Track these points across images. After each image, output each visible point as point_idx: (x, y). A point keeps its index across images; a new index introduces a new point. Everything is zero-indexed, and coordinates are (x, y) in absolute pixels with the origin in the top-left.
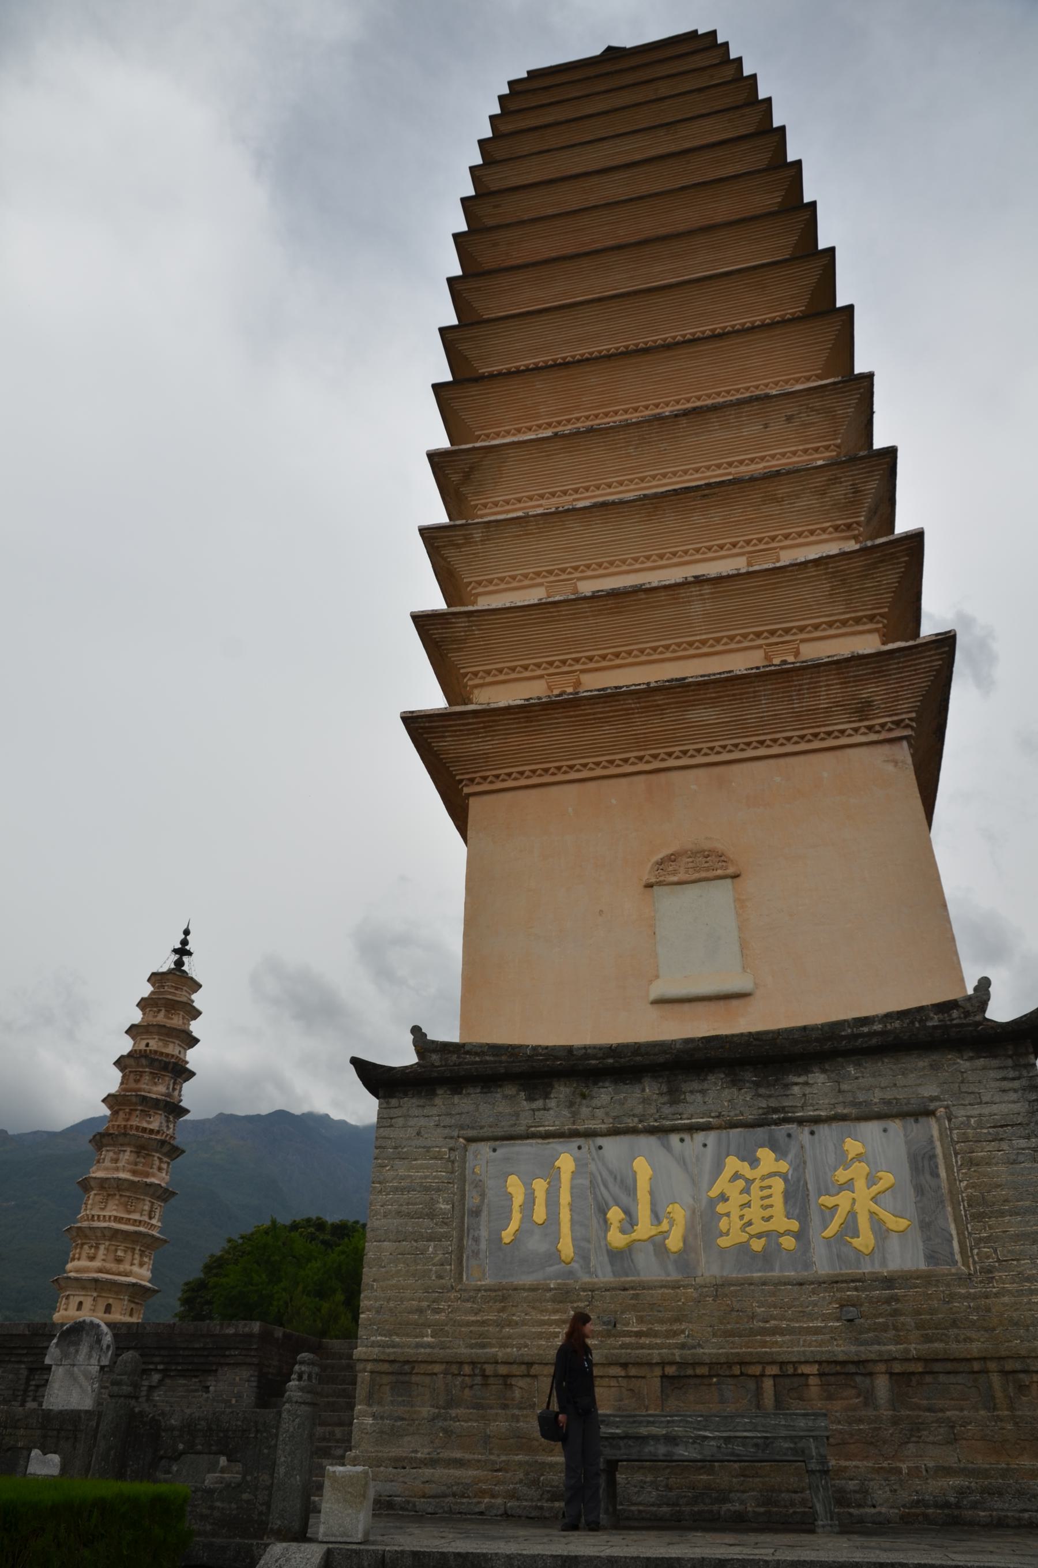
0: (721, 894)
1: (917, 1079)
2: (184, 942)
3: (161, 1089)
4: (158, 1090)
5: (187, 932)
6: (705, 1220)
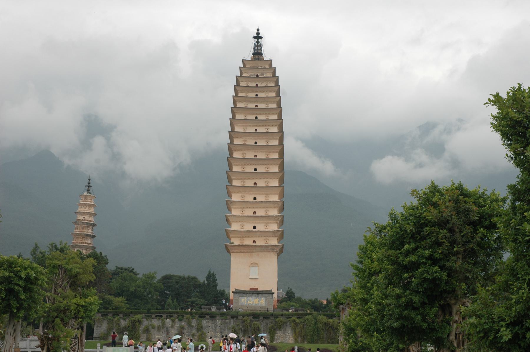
0: (257, 268)
1: (267, 295)
2: (89, 183)
3: (90, 231)
4: (89, 232)
5: (89, 180)
6: (254, 302)
